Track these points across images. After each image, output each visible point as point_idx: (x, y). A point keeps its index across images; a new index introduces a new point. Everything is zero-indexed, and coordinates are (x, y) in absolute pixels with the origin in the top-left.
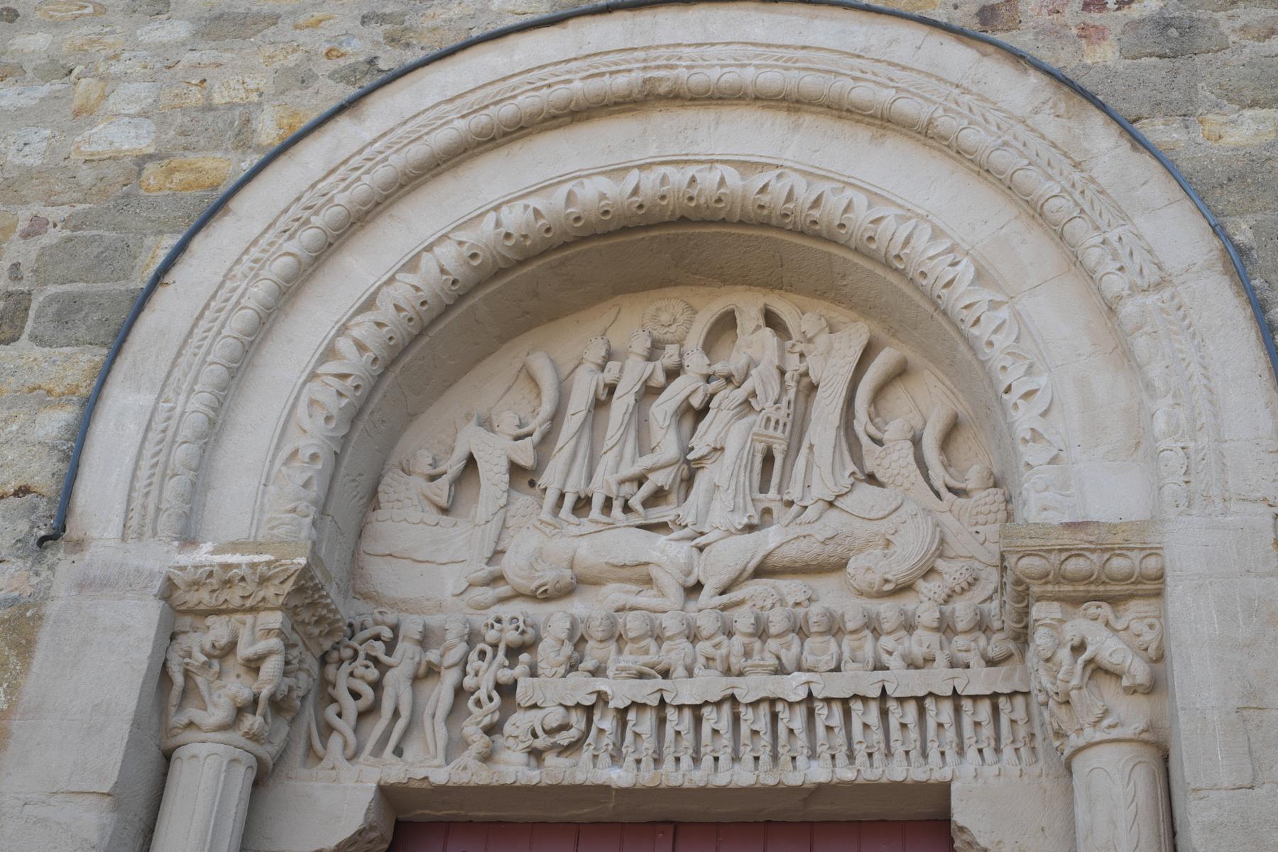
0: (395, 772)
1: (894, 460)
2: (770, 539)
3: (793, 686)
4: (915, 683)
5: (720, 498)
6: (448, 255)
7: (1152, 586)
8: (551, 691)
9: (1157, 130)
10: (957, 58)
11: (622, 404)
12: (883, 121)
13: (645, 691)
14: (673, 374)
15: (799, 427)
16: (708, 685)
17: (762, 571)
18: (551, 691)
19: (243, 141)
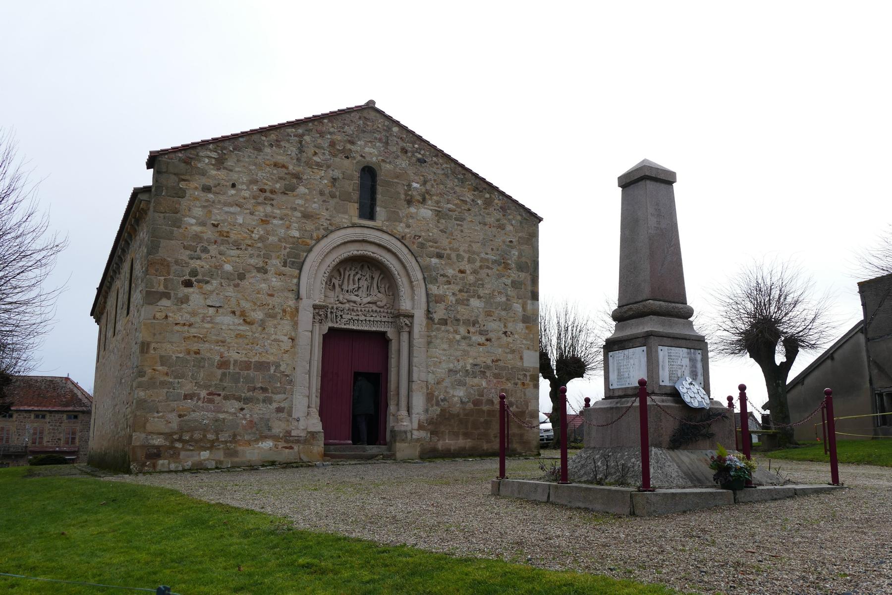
0: (331, 325)
1: (382, 290)
2: (369, 299)
3: (372, 319)
4: (384, 319)
5: (363, 293)
6: (338, 260)
7: (412, 316)
8: (347, 317)
9: (419, 259)
10: (399, 244)
11: (351, 277)
12: (389, 250)
13: (356, 318)
14: (357, 273)
15: (372, 283)
16: (363, 318)
17: (369, 303)
18: (347, 317)
19: (312, 238)
